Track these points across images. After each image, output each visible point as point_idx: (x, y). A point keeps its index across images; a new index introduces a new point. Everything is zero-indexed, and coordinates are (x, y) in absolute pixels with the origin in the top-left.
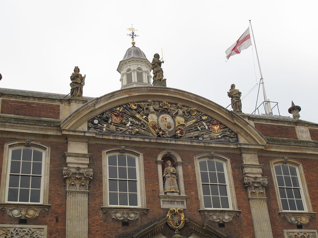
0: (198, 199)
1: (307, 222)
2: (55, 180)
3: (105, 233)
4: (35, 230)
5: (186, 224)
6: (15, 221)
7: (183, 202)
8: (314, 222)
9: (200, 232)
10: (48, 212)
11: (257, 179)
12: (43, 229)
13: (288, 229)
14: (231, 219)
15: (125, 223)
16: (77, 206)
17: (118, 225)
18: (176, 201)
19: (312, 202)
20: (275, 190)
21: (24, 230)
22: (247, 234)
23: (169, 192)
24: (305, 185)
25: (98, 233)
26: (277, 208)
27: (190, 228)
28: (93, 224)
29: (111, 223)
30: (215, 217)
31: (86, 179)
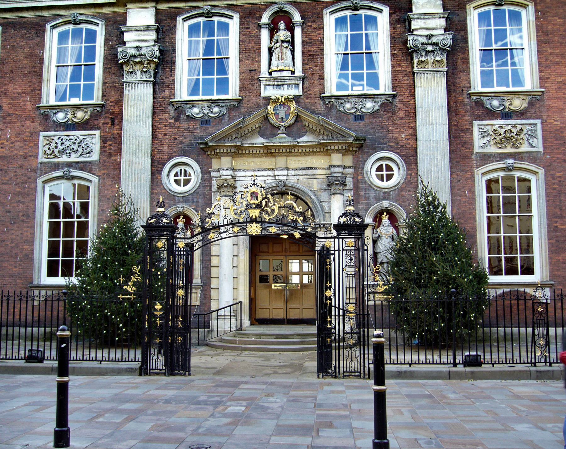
0: (323, 79)
2: (110, 68)
3: (176, 136)
4: (85, 137)
7: (297, 85)
8: (538, 106)
10: (101, 112)
11: (434, 38)
14: (377, 108)
16: (137, 101)
19: (540, 71)
21: (71, 137)
22: (402, 130)
26: (468, 85)
30: (348, 106)
31: (150, 62)
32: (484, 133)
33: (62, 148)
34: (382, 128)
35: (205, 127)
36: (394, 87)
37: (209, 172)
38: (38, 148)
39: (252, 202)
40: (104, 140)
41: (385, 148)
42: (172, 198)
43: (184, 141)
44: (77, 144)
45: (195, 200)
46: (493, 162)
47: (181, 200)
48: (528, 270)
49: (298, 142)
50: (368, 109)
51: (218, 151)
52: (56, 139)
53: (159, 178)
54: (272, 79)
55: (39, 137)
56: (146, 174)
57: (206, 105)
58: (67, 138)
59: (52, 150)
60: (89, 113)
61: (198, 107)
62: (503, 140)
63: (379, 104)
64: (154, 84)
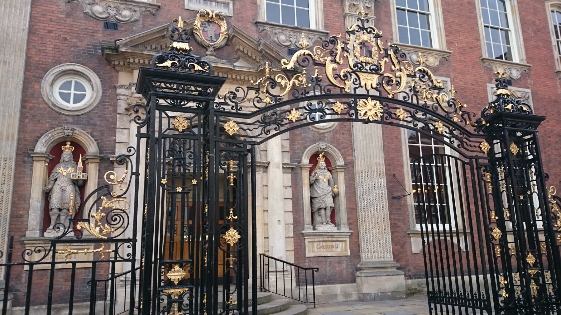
1: (436, 64)
5: (229, 40)
9: (254, 57)
15: (111, 25)
17: (95, 26)
19: (447, 36)
20: (390, 9)
24: (439, 9)
25: (51, 34)
26: (391, 37)
27: (237, 47)
28: (42, 19)
29: (81, 21)
30: (282, 37)
35: (109, 31)
36: (326, 27)
37: (115, 88)
39: (362, 59)
42: (56, 115)
43: (79, 44)
45: (91, 122)
47: (70, 120)
48: (445, 219)
49: (234, 66)
51: (132, 60)
56: (16, 79)
61: (102, 6)
63: (313, 40)
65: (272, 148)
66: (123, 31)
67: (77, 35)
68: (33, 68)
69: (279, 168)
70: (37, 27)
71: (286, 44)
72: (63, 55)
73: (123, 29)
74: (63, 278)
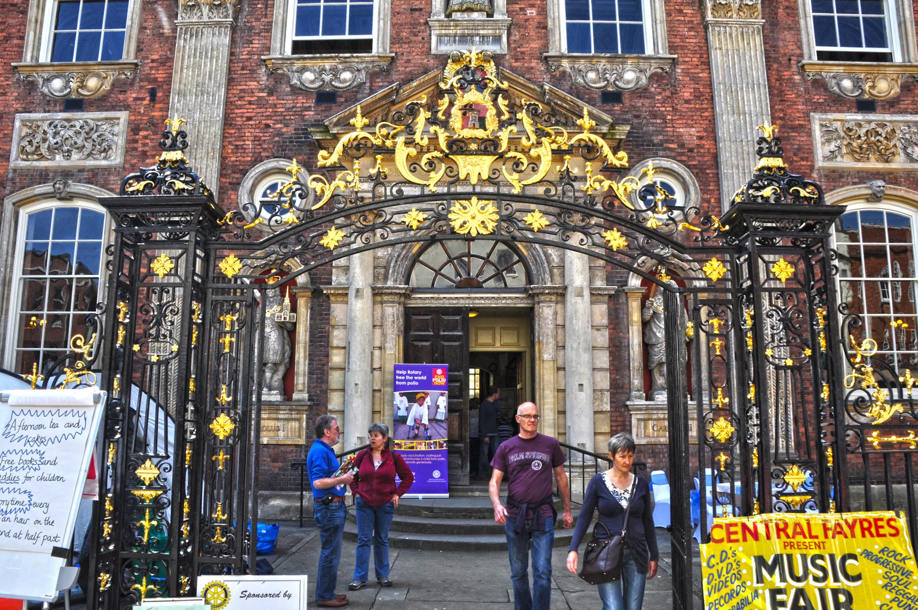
0: (545, 27)
3: (268, 122)
6: (55, 105)
7: (497, 39)
12: (119, 119)
13: (826, 112)
16: (201, 58)
18: (478, 35)
22: (689, 122)
23: (458, 11)
25: (250, 122)
26: (798, 52)
28: (239, 103)
30: (592, 75)
32: (829, 134)
33: (55, 141)
34: (655, 116)
36: (672, 48)
38: (11, 141)
40: (134, 128)
41: (661, 153)
43: (284, 130)
44: (83, 135)
46: (848, 184)
50: (628, 82)
52: (45, 126)
53: (233, 197)
54: (452, 23)
55: (13, 122)
57: (328, 67)
58: (66, 124)
59: (35, 144)
60: (110, 79)
62: (864, 146)
63: (648, 74)
64: (234, 29)
65: (571, 262)
66: (342, 103)
67: (281, 118)
68: (229, 172)
69: (582, 296)
70: (234, 115)
71: (598, 85)
72: (264, 149)
73: (343, 100)
74: (270, 456)
